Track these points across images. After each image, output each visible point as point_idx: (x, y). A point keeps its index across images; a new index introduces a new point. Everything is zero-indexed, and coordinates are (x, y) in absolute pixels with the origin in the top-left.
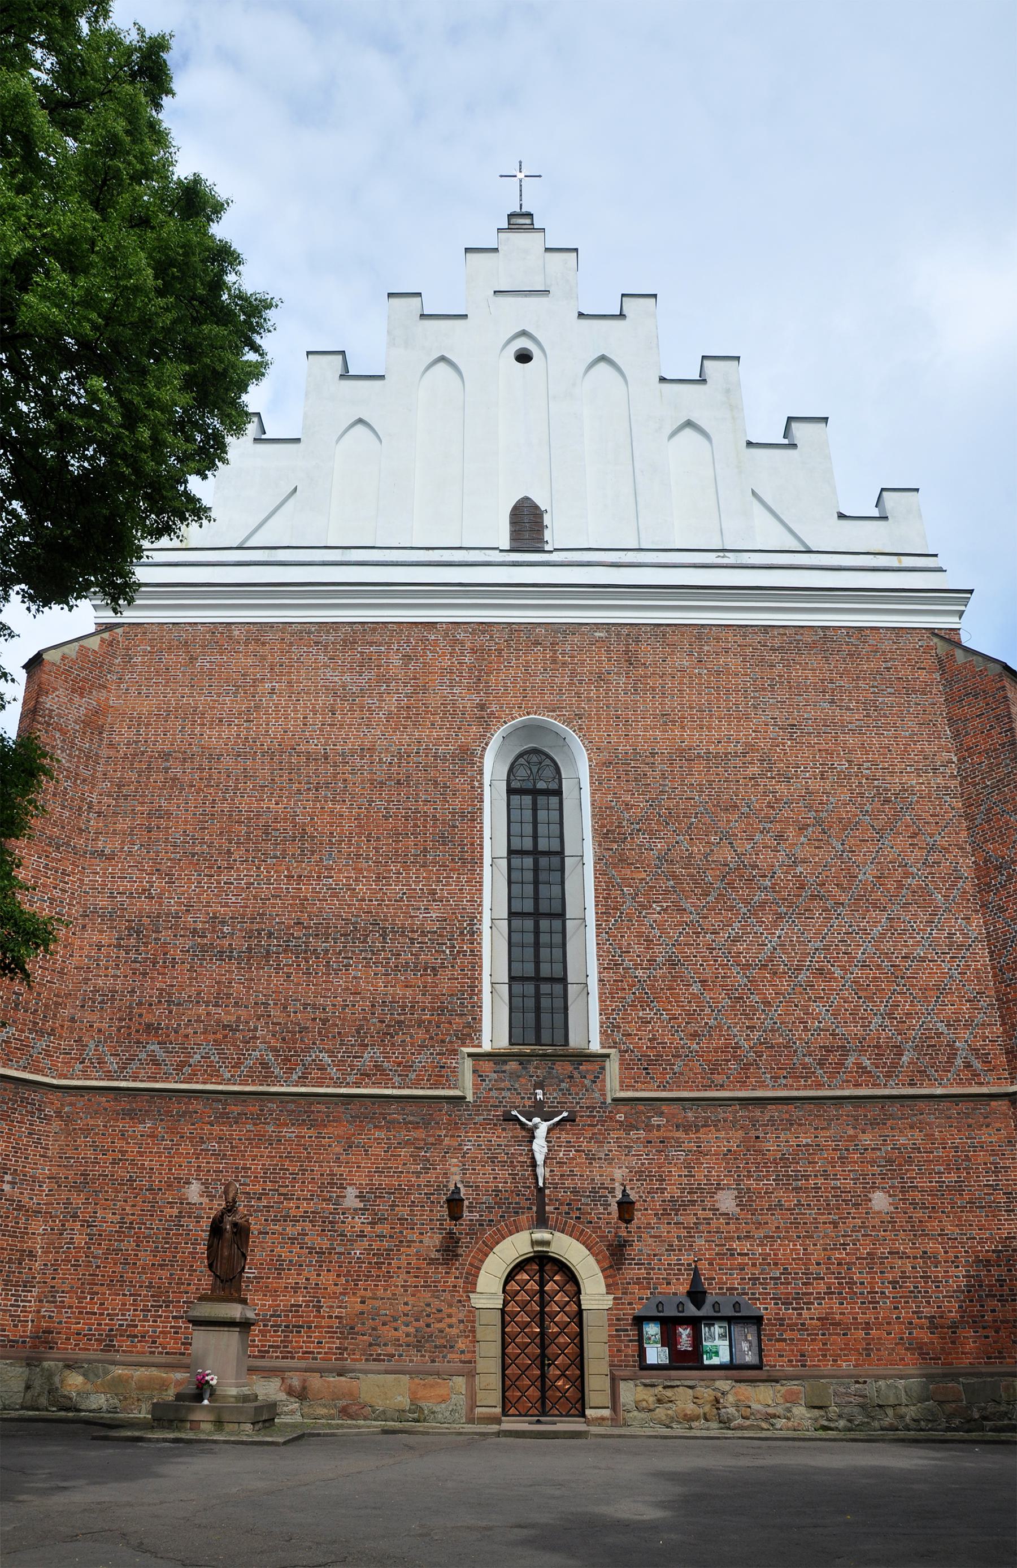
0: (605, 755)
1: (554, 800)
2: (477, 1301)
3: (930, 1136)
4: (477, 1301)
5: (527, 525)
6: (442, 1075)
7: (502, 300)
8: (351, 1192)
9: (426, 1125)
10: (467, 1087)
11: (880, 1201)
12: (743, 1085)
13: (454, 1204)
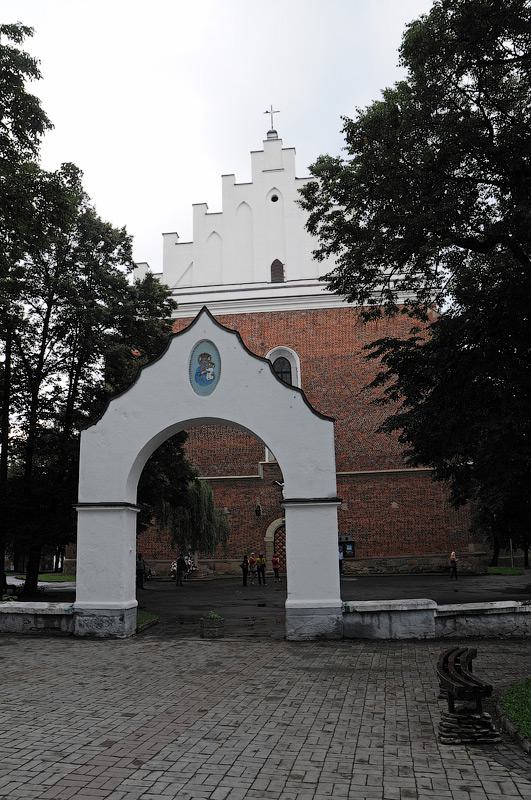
0: (305, 360)
1: (288, 375)
2: (266, 540)
3: (413, 484)
4: (266, 540)
5: (277, 269)
6: (254, 471)
7: (266, 174)
8: (226, 509)
9: (249, 487)
10: (261, 474)
11: (394, 505)
12: (351, 470)
13: (258, 512)
